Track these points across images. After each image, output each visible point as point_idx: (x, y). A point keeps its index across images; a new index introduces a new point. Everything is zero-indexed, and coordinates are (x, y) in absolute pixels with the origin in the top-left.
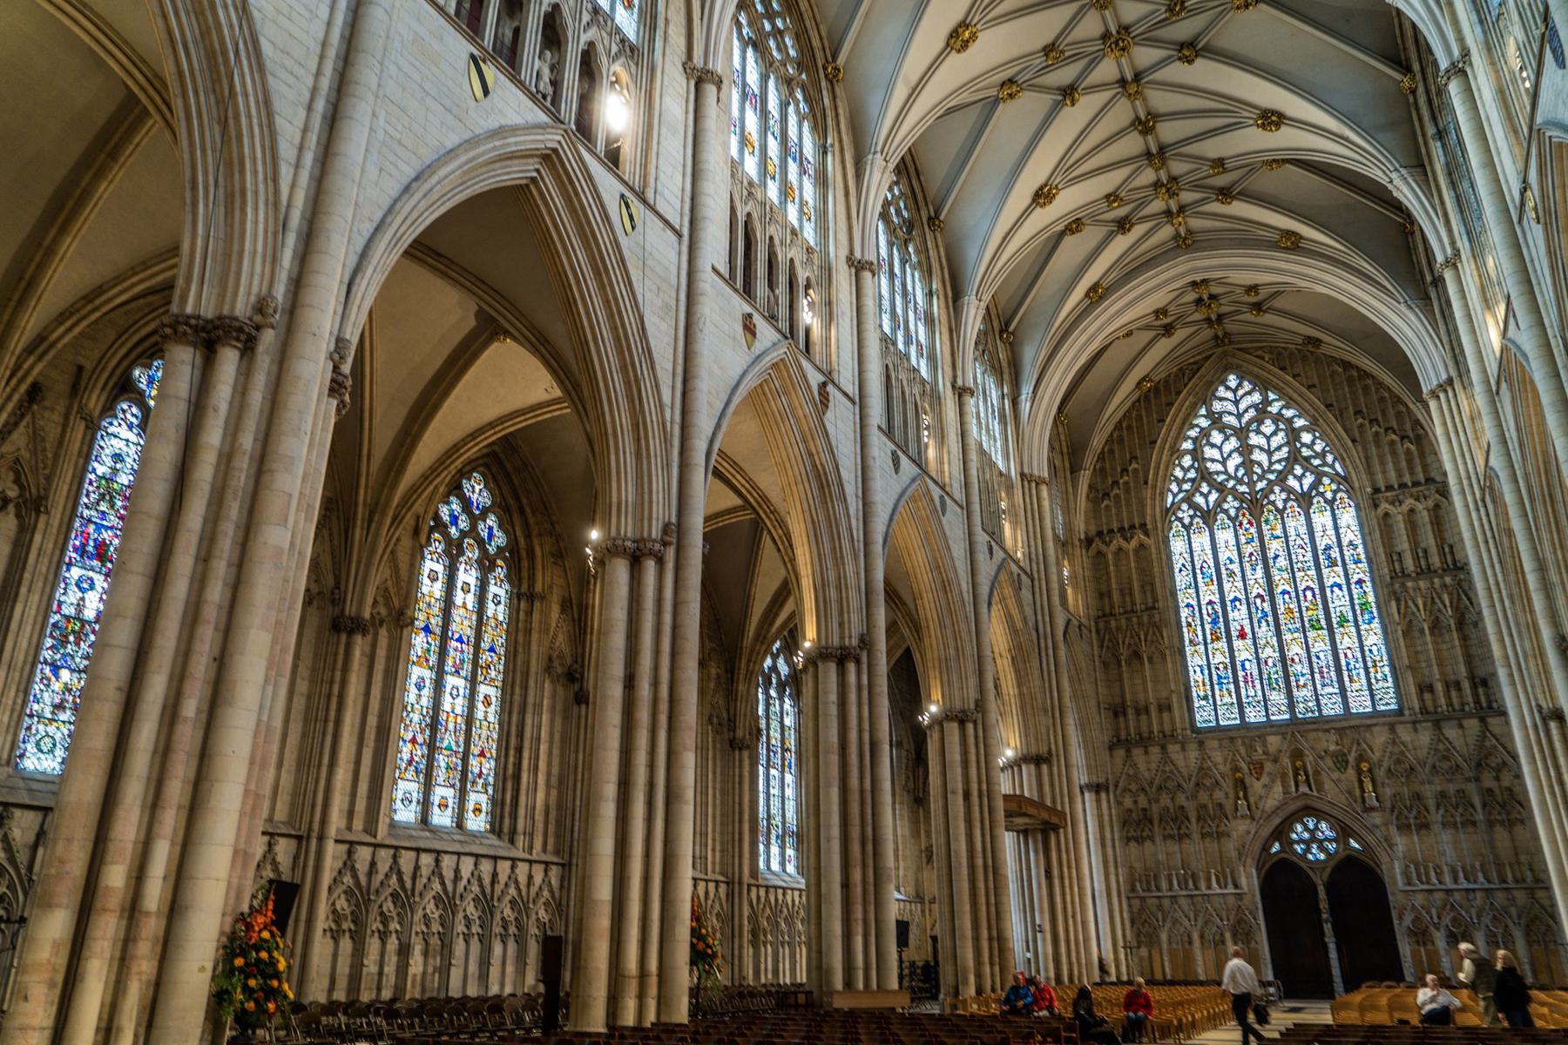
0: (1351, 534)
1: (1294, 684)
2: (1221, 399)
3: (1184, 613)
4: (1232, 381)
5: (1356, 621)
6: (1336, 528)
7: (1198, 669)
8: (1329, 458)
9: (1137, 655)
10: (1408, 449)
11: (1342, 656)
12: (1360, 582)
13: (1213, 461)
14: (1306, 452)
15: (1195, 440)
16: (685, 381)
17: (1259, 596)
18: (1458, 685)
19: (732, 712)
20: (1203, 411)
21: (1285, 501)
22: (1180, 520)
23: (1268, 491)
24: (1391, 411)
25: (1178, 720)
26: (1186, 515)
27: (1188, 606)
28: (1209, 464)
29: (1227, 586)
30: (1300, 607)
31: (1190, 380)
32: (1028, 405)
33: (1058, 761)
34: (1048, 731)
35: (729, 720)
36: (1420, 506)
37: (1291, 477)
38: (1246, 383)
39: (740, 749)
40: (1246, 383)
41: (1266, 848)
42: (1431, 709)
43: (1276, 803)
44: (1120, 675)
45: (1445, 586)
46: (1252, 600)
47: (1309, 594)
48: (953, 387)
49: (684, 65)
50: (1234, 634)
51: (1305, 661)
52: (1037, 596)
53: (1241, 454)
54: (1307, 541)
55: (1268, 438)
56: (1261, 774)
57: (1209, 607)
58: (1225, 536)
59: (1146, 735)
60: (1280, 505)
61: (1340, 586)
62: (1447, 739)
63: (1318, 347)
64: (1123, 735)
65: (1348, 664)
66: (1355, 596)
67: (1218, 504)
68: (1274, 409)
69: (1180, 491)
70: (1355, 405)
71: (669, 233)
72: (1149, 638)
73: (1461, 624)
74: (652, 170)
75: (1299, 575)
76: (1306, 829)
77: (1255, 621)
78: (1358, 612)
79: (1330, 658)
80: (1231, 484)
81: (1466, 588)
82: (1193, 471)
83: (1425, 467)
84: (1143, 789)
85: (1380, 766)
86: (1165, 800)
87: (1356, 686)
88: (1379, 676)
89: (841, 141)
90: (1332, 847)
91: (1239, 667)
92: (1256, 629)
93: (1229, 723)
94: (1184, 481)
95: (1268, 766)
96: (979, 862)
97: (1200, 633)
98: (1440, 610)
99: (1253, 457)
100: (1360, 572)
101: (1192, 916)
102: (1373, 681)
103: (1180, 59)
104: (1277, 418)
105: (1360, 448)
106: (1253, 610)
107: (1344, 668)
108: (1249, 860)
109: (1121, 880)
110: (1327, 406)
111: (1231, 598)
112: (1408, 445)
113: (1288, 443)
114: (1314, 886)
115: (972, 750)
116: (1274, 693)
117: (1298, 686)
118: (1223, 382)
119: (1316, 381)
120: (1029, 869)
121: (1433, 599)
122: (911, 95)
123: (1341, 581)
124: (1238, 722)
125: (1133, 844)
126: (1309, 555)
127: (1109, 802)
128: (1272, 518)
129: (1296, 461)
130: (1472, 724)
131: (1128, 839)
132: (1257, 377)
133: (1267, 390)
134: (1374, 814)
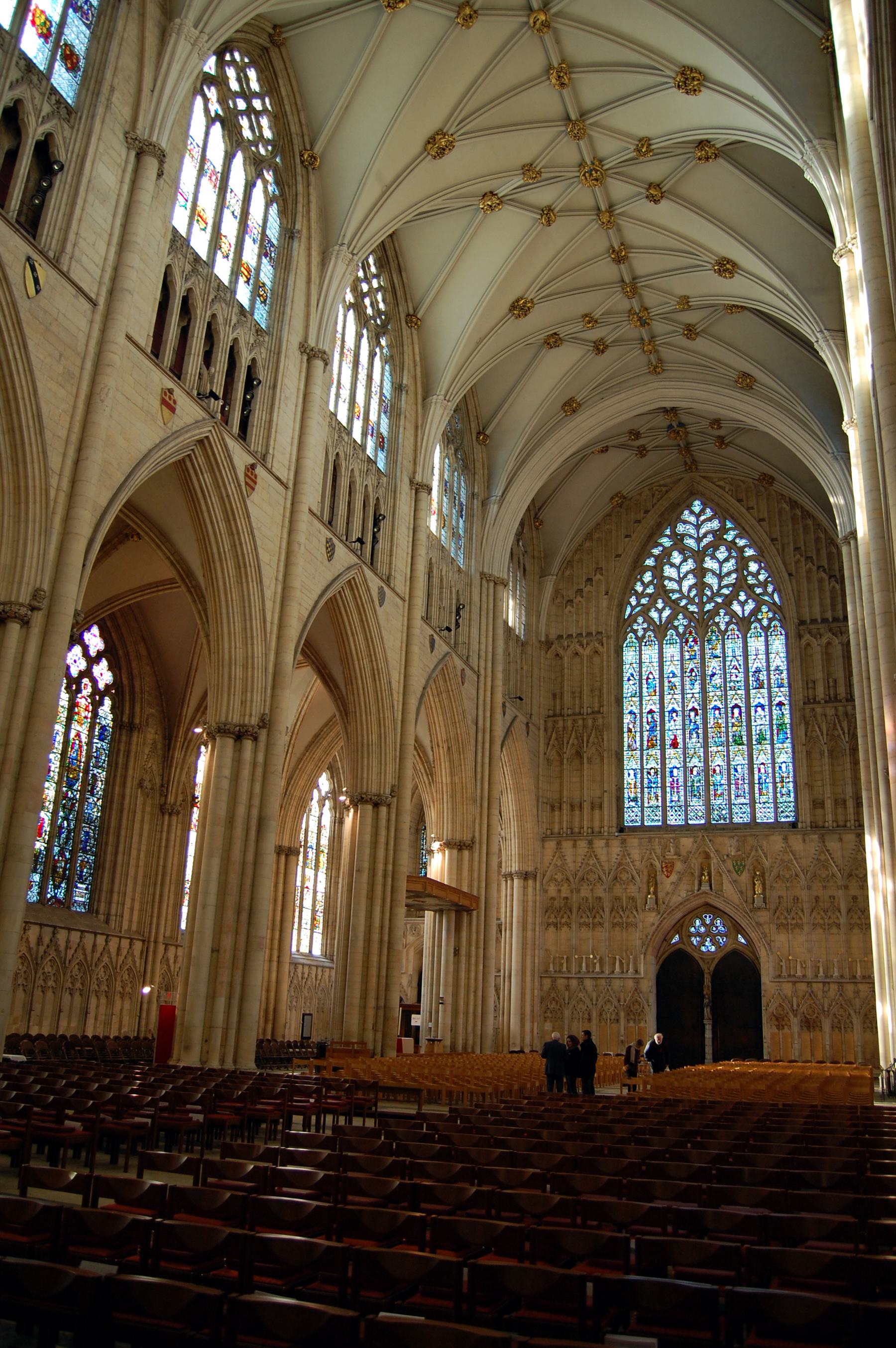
0: (779, 661)
1: (712, 793)
2: (685, 522)
3: (627, 719)
4: (697, 506)
5: (772, 739)
6: (767, 654)
7: (632, 772)
8: (770, 589)
9: (579, 754)
10: (834, 587)
12: (780, 704)
13: (671, 579)
14: (751, 580)
15: (657, 558)
16: (80, 450)
17: (694, 709)
18: (845, 801)
19: (166, 779)
20: (668, 532)
21: (728, 624)
22: (635, 632)
23: (715, 612)
24: (824, 552)
25: (606, 818)
26: (640, 627)
27: (631, 713)
28: (666, 582)
29: (667, 698)
30: (727, 722)
32: (496, 506)
33: (480, 848)
34: (474, 822)
35: (162, 786)
37: (735, 602)
38: (708, 510)
39: (170, 815)
40: (708, 510)
41: (666, 939)
43: (680, 899)
44: (562, 772)
46: (687, 713)
47: (736, 711)
48: (411, 482)
49: (126, 133)
50: (668, 742)
51: (725, 772)
52: (481, 692)
54: (741, 662)
55: (721, 563)
56: (671, 872)
57: (650, 716)
58: (672, 651)
59: (577, 830)
60: (723, 627)
61: (762, 707)
62: (828, 850)
63: (771, 484)
64: (556, 830)
65: (760, 778)
66: (775, 717)
68: (729, 537)
69: (638, 604)
70: (795, 542)
71: (82, 300)
72: (591, 740)
74: (72, 236)
75: (730, 693)
76: (703, 924)
77: (687, 732)
78: (775, 732)
80: (683, 603)
82: (652, 587)
84: (567, 879)
85: (771, 871)
86: (585, 892)
87: (764, 799)
88: (784, 791)
89: (309, 228)
90: (722, 940)
91: (668, 774)
92: (687, 740)
93: (653, 824)
94: (642, 595)
95: (679, 866)
96: (376, 937)
97: (638, 739)
99: (705, 580)
100: (782, 695)
102: (779, 795)
103: (647, 197)
104: (732, 544)
105: (794, 581)
106: (687, 722)
107: (756, 782)
108: (650, 949)
110: (773, 540)
111: (670, 709)
112: (833, 583)
113: (736, 571)
114: (702, 974)
115: (383, 832)
116: (695, 799)
117: (715, 795)
118: (689, 507)
119: (766, 515)
120: (440, 946)
121: (835, 724)
122: (385, 193)
123: (764, 702)
124: (660, 823)
125: (552, 929)
126: (741, 675)
128: (714, 638)
129: (741, 589)
131: (549, 925)
132: (718, 505)
134: (759, 913)
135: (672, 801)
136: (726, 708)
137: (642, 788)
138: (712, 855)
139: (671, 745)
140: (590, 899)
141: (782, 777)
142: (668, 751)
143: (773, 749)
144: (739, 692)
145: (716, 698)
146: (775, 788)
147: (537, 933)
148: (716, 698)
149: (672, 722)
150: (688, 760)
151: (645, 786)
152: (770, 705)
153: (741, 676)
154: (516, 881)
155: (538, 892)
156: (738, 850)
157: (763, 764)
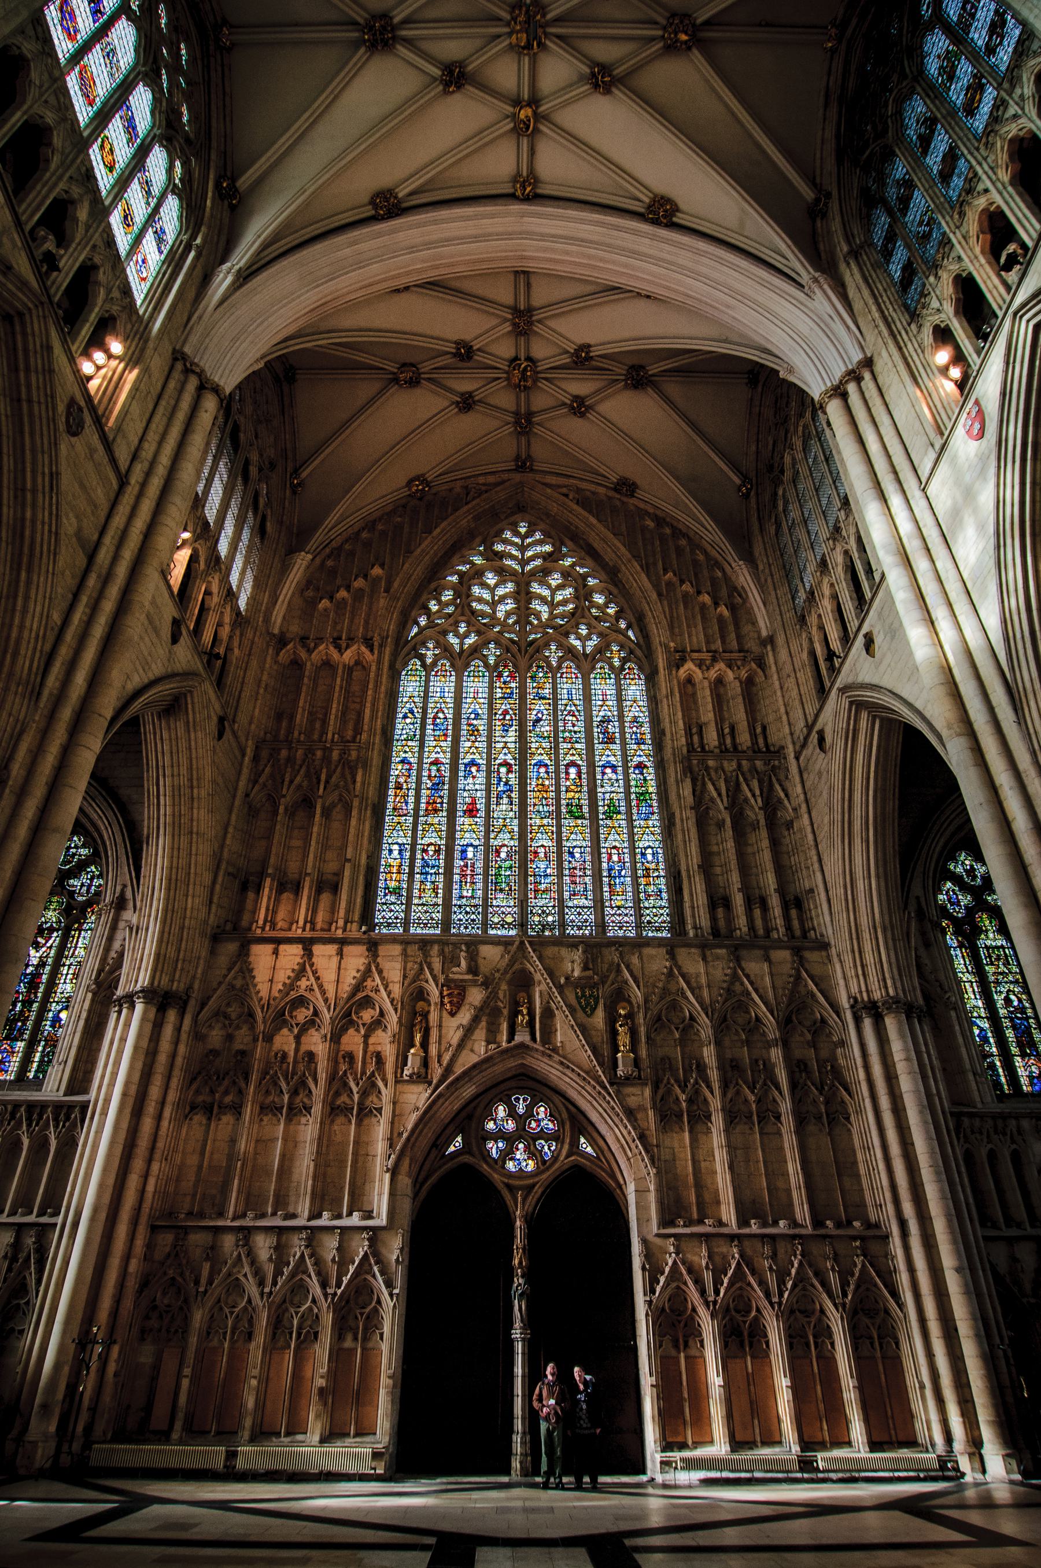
2: (506, 542)
3: (396, 770)
6: (620, 699)
7: (396, 847)
8: (623, 625)
9: (307, 803)
11: (604, 857)
12: (640, 766)
13: (480, 600)
15: (461, 575)
17: (505, 764)
22: (422, 658)
27: (403, 762)
28: (474, 604)
30: (558, 785)
31: (474, 499)
36: (730, 675)
42: (723, 931)
44: (271, 830)
45: (754, 769)
47: (573, 771)
50: (461, 808)
51: (553, 857)
53: (517, 601)
58: (476, 686)
65: (610, 870)
66: (633, 783)
67: (475, 651)
68: (568, 562)
69: (431, 625)
72: (334, 779)
73: (772, 824)
76: (512, 1113)
77: (494, 794)
78: (634, 803)
79: (588, 858)
81: (782, 777)
83: (739, 638)
87: (618, 901)
91: (457, 855)
95: (476, 996)
97: (411, 800)
98: (746, 800)
100: (643, 754)
101: (269, 1269)
109: (150, 1188)
116: (500, 896)
117: (536, 891)
119: (623, 528)
121: (738, 784)
126: (581, 724)
127: (178, 1029)
130: (783, 956)
131: (193, 1108)
133: (563, 543)
135: (461, 897)
136: (557, 765)
137: (411, 874)
138: (537, 977)
139: (465, 812)
140: (292, 1054)
141: (647, 869)
142: (460, 820)
143: (631, 826)
144: (577, 746)
145: (540, 751)
146: (636, 884)
147: (165, 1123)
148: (540, 751)
149: (470, 780)
150: (492, 836)
151: (417, 870)
152: (626, 768)
153: (580, 726)
154: (139, 1007)
155: (184, 1036)
156: (585, 968)
157: (615, 847)
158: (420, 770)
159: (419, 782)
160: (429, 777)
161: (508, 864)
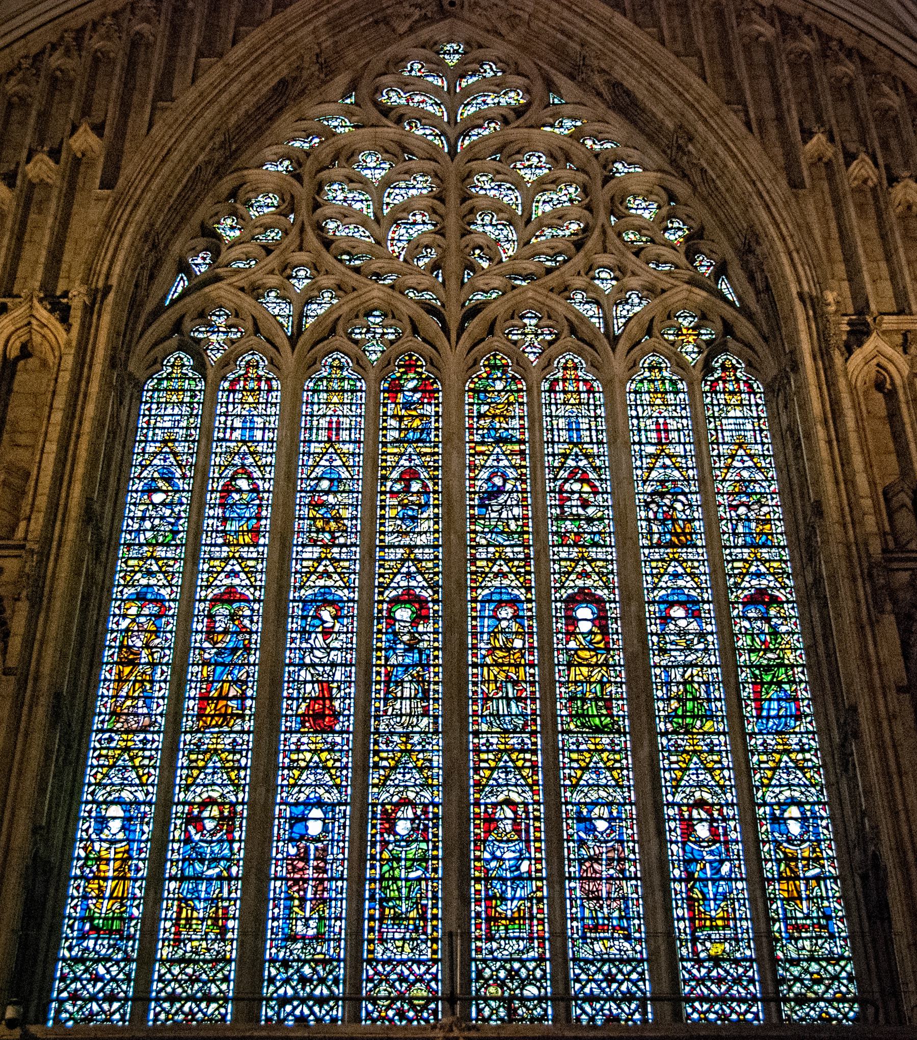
8: (705, 267)
12: (761, 598)
17: (408, 598)
22: (197, 350)
26: (214, 338)
27: (140, 597)
51: (539, 830)
66: (743, 642)
77: (379, 675)
78: (748, 691)
79: (630, 831)
91: (280, 829)
97: (162, 690)
111: (305, 593)
133: (550, 86)
136: (544, 599)
137: (156, 881)
143: (742, 752)
144: (593, 552)
158: (186, 616)
159: (183, 648)
160: (210, 632)
161: (412, 851)
